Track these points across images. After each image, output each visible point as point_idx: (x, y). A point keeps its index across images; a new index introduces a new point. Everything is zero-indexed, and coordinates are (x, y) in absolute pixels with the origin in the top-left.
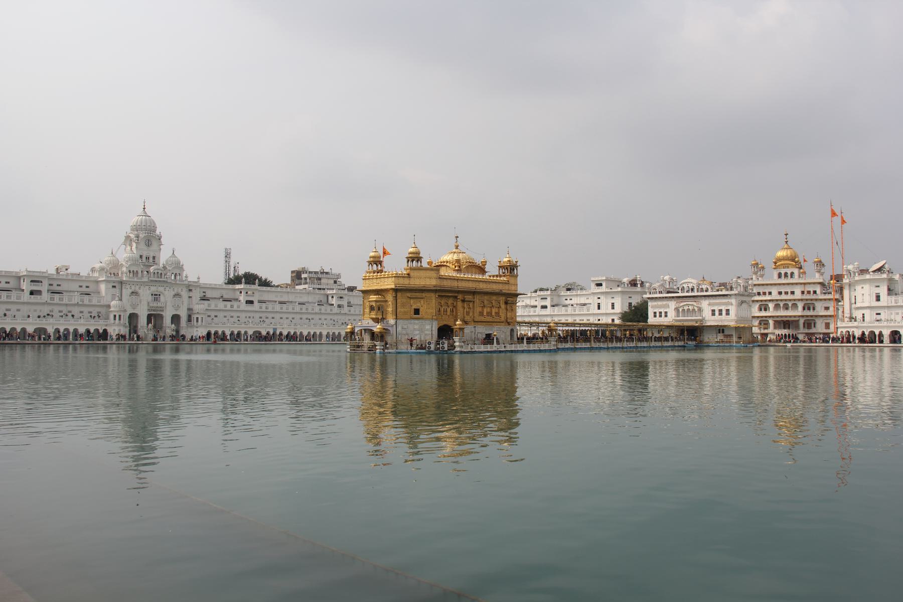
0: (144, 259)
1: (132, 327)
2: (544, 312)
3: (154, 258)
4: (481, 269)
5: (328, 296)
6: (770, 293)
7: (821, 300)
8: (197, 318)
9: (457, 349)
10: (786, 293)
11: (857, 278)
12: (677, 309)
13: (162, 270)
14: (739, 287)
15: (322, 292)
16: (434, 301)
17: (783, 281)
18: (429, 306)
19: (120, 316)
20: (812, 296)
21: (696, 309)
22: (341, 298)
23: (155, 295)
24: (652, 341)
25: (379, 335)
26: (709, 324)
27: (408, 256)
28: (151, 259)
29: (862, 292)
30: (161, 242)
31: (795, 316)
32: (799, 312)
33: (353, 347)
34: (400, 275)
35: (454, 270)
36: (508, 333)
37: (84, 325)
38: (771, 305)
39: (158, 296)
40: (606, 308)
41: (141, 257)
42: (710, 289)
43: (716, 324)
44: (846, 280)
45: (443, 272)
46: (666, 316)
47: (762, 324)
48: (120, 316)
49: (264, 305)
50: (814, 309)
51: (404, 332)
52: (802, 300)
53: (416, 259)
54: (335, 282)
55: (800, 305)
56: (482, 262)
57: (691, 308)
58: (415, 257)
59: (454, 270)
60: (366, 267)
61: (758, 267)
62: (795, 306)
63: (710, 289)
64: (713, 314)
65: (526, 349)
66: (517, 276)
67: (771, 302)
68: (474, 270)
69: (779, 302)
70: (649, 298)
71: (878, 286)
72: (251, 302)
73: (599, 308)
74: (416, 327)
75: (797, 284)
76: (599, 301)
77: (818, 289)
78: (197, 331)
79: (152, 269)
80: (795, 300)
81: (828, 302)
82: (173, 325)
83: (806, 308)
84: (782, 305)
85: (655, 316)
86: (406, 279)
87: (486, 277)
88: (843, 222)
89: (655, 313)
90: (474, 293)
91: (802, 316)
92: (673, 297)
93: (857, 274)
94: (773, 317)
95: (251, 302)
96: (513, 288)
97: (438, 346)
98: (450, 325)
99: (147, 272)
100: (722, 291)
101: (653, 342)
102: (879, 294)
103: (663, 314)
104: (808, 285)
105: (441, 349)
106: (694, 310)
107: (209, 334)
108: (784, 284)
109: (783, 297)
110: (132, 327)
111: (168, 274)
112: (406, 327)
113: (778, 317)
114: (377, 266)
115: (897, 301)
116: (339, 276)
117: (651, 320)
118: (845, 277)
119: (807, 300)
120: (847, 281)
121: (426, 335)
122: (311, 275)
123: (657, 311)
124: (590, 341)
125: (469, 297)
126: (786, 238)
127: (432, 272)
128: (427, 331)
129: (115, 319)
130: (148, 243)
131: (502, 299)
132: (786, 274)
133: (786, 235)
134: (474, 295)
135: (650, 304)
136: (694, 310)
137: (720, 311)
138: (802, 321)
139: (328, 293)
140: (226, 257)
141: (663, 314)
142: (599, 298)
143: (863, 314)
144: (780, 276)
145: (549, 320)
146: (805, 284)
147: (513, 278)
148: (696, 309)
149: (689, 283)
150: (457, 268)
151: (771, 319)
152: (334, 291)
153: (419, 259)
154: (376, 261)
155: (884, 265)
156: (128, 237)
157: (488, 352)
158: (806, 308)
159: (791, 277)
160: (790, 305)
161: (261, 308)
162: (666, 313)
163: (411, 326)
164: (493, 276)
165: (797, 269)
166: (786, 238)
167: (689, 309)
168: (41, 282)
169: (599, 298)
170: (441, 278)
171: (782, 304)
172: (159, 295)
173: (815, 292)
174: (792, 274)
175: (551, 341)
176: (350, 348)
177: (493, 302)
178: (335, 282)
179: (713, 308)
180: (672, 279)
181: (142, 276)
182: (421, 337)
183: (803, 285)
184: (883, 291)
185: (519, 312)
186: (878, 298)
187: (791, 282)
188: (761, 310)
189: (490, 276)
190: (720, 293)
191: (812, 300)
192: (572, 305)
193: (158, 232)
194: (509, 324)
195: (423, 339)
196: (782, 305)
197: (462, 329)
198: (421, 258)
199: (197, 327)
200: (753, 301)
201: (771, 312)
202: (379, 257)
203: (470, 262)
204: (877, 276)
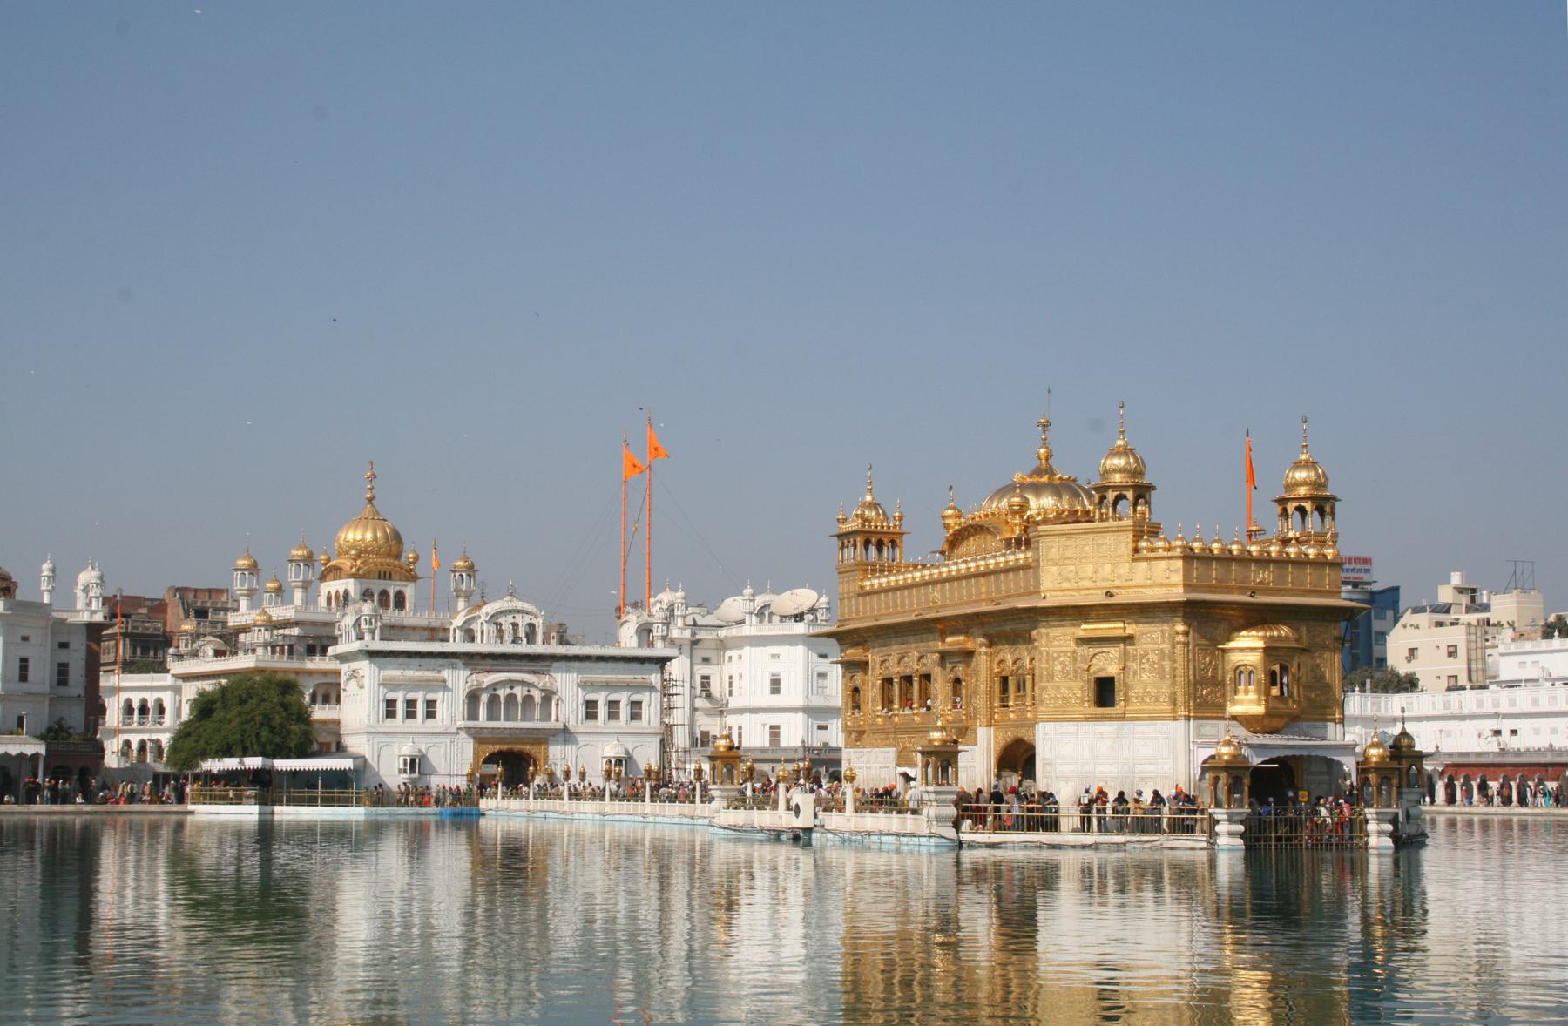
12: (473, 698)
21: (537, 695)
46: (431, 714)
57: (519, 692)
64: (591, 714)
103: (420, 709)
106: (528, 699)
136: (528, 699)
137: (411, 704)
141: (420, 709)
148: (537, 695)
149: (519, 612)
162: (431, 704)
167: (511, 698)
179: (591, 697)
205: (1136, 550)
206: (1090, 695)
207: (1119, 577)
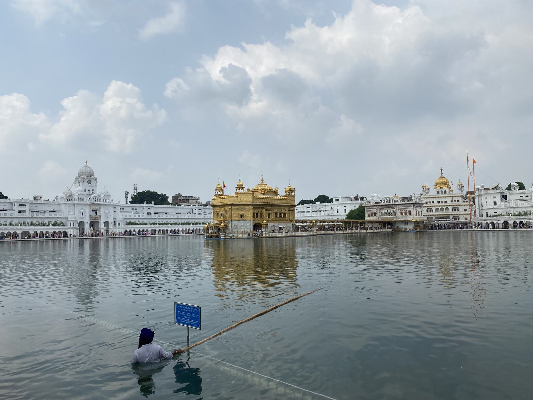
0: (87, 191)
1: (81, 229)
2: (308, 215)
3: (93, 190)
4: (275, 193)
5: (193, 209)
6: (433, 202)
7: (462, 205)
8: (119, 223)
9: (264, 236)
10: (442, 202)
11: (483, 193)
13: (98, 197)
14: (416, 199)
15: (190, 207)
16: (251, 210)
17: (440, 195)
18: (249, 213)
19: (74, 223)
20: (457, 203)
22: (200, 210)
23: (94, 211)
24: (368, 229)
25: (222, 229)
26: (399, 220)
27: (237, 186)
28: (91, 192)
29: (486, 201)
30: (97, 181)
31: (447, 215)
32: (450, 212)
33: (208, 236)
34: (233, 197)
35: (261, 194)
36: (291, 226)
37: (52, 229)
38: (434, 209)
39: (96, 212)
40: (342, 212)
41: (85, 190)
42: (399, 201)
43: (403, 219)
44: (476, 194)
45: (256, 195)
46: (375, 216)
47: (429, 219)
48: (74, 223)
49: (157, 215)
50: (458, 210)
51: (236, 227)
52: (451, 205)
53: (241, 188)
54: (197, 202)
55: (450, 208)
56: (276, 189)
57: (389, 211)
58: (241, 187)
59: (261, 194)
60: (214, 193)
61: (425, 189)
62: (447, 209)
63: (399, 201)
65: (300, 234)
66: (294, 196)
67: (434, 207)
68: (272, 193)
69: (438, 207)
70: (365, 206)
71: (495, 197)
72: (150, 213)
73: (338, 212)
74: (242, 224)
75: (448, 197)
76: (338, 208)
77: (460, 199)
78: (119, 230)
79: (92, 196)
80: (447, 206)
81: (466, 206)
82: (105, 227)
83: (454, 210)
84: (440, 209)
85: (369, 216)
86: (236, 199)
87: (278, 197)
88: (474, 162)
89: (369, 214)
90: (272, 206)
91: (452, 215)
92: (378, 206)
93: (483, 191)
94: (435, 215)
95: (150, 213)
96: (292, 202)
97: (254, 234)
98: (260, 223)
99: (89, 198)
100: (405, 201)
102: (496, 201)
104: (454, 197)
105: (255, 236)
107: (126, 231)
108: (441, 197)
109: (441, 204)
110: (81, 229)
111: (102, 199)
112: (236, 224)
113: (437, 215)
114: (220, 192)
115: (506, 205)
116: (198, 198)
117: (367, 218)
118: (476, 192)
119: (454, 205)
120: (477, 195)
121: (247, 228)
122: (183, 198)
123: (370, 213)
124: (334, 230)
125: (269, 208)
126: (442, 172)
127: (249, 195)
128: (247, 226)
129: (71, 225)
130: (89, 182)
131: (287, 209)
133: (441, 170)
134: (272, 207)
135: (366, 209)
138: (451, 217)
139: (193, 207)
140: (135, 189)
142: (338, 207)
143: (487, 213)
144: (438, 192)
145: (311, 219)
146: (453, 197)
147: (293, 197)
150: (263, 193)
151: (434, 216)
152: (197, 206)
153: (243, 188)
154: (219, 190)
155: (498, 185)
156: (77, 179)
157: (281, 237)
158: (454, 210)
159: (445, 193)
160: (444, 209)
161: (155, 216)
163: (239, 224)
164: (282, 196)
165: (448, 189)
166: (442, 172)
168: (25, 205)
169: (338, 207)
170: (254, 198)
171: (440, 208)
172: (97, 211)
173: (458, 201)
174: (445, 192)
175: (313, 230)
176: (207, 237)
177: (283, 210)
178: (197, 202)
180: (378, 196)
181: (86, 201)
182: (244, 230)
183: (451, 197)
184: (498, 199)
185: (296, 215)
186: (495, 203)
187: (445, 196)
188: (428, 211)
189: (280, 196)
190: (404, 203)
191: (457, 205)
192: (323, 211)
193: (95, 176)
194: (291, 221)
195: (245, 230)
196: (440, 209)
197: (266, 225)
198: (244, 187)
199: (119, 228)
200: (423, 207)
201: (434, 213)
202: (221, 188)
203: (269, 189)
204: (495, 191)
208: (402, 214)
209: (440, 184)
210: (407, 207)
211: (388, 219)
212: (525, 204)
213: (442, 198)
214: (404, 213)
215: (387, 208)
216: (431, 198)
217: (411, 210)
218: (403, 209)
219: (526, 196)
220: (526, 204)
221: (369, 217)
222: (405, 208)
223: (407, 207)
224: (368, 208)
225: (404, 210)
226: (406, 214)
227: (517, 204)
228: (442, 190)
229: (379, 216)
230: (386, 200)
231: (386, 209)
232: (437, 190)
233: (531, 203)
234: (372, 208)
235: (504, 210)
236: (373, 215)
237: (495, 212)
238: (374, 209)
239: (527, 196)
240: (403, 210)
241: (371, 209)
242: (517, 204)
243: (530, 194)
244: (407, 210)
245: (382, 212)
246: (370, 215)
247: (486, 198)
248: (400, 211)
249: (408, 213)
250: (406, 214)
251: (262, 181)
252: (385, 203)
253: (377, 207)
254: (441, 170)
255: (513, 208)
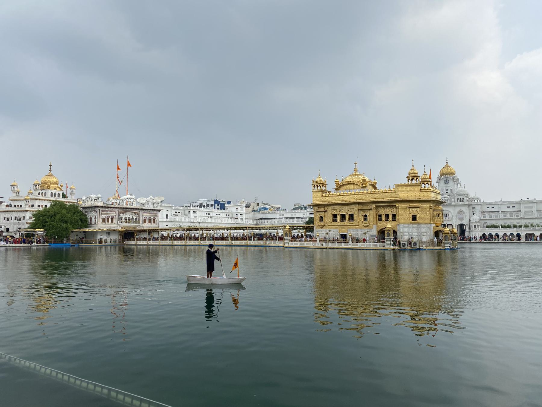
46: (112, 221)
57: (131, 217)
85: (104, 221)
92: (119, 208)
101: (151, 241)
102: (168, 214)
123: (105, 217)
126: (50, 168)
132: (55, 194)
133: (50, 166)
136: (133, 218)
149: (131, 198)
166: (50, 168)
186: (167, 217)
205: (421, 190)
206: (411, 219)
207: (417, 195)
208: (145, 222)
209: (54, 184)
210: (152, 213)
211: (129, 227)
212: (186, 220)
213: (41, 201)
214: (147, 221)
215: (130, 213)
216: (45, 200)
217: (156, 217)
218: (148, 215)
219: (179, 212)
220: (187, 220)
221: (104, 223)
222: (150, 214)
223: (152, 214)
224: (104, 209)
225: (149, 217)
226: (150, 222)
227: (181, 219)
228: (56, 192)
229: (118, 222)
230: (128, 200)
231: (127, 213)
232: (51, 192)
233: (190, 219)
234: (110, 209)
235: (173, 223)
236: (110, 220)
237: (167, 225)
238: (112, 211)
239: (179, 212)
240: (148, 217)
241: (108, 211)
242: (181, 219)
243: (181, 211)
244: (151, 217)
245: (122, 219)
246: (106, 221)
247: (167, 211)
248: (145, 217)
249: (152, 221)
250: (150, 222)
251: (356, 171)
252: (129, 206)
253: (117, 210)
254: (50, 166)
255: (179, 222)
